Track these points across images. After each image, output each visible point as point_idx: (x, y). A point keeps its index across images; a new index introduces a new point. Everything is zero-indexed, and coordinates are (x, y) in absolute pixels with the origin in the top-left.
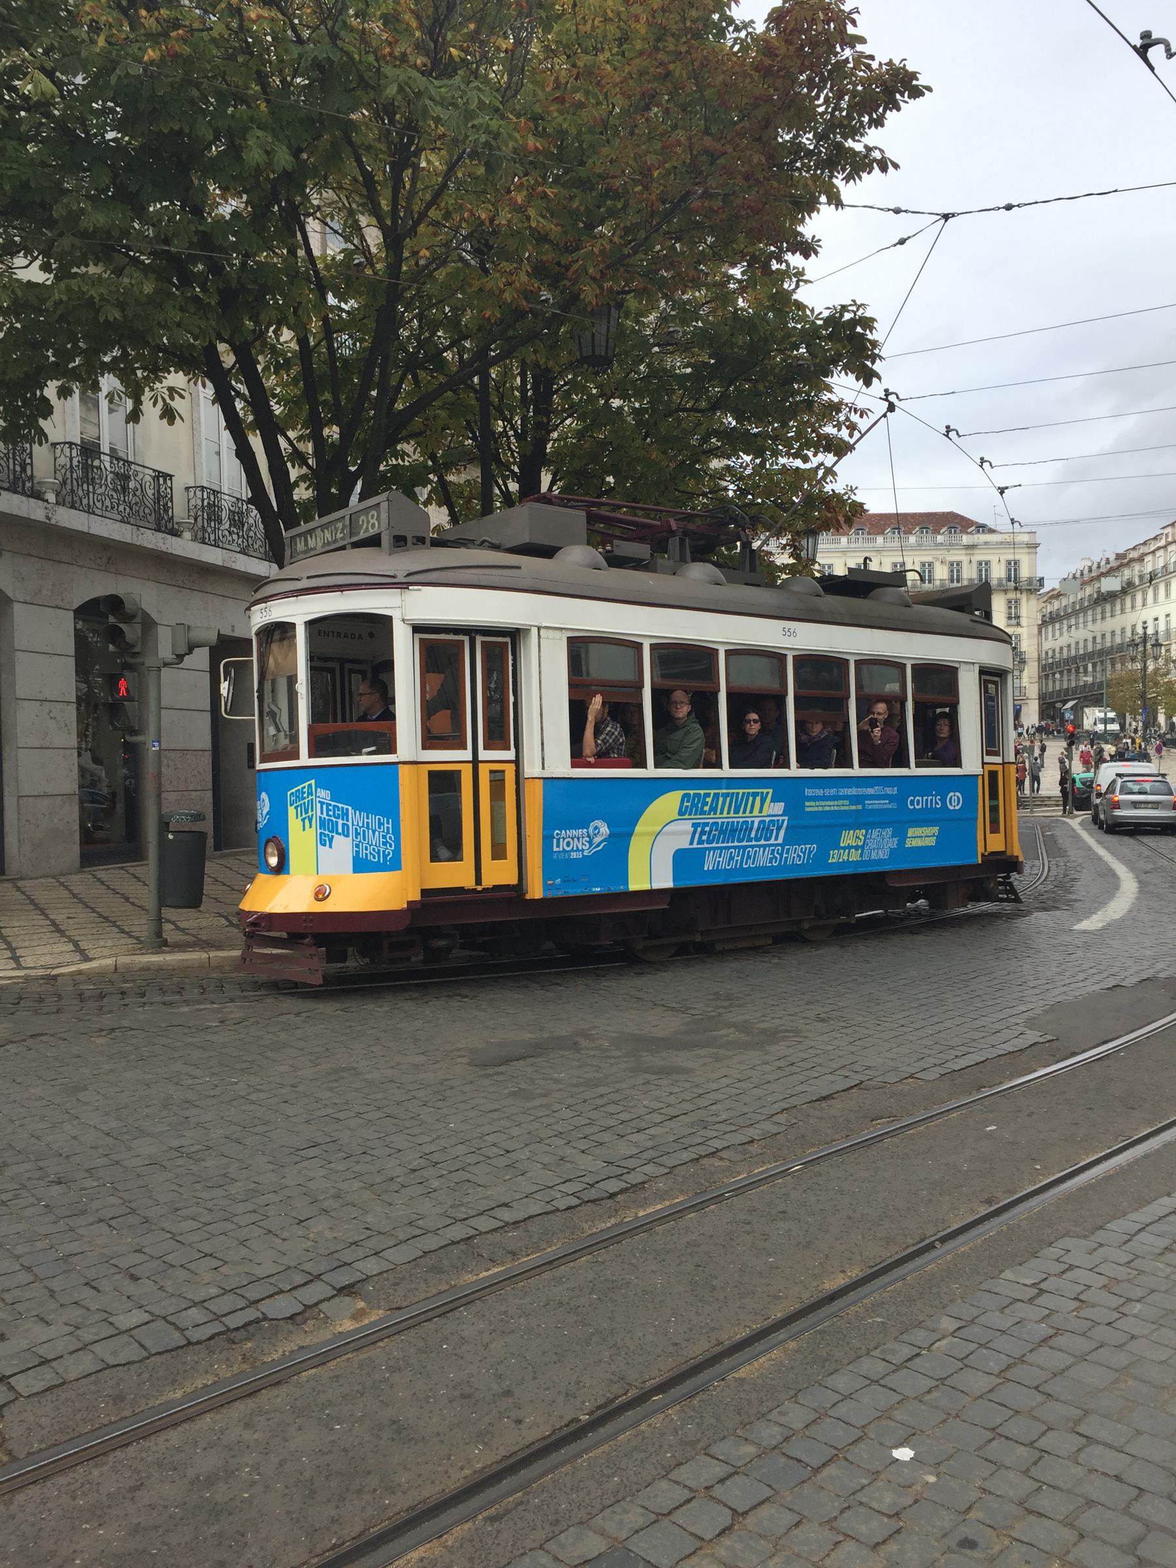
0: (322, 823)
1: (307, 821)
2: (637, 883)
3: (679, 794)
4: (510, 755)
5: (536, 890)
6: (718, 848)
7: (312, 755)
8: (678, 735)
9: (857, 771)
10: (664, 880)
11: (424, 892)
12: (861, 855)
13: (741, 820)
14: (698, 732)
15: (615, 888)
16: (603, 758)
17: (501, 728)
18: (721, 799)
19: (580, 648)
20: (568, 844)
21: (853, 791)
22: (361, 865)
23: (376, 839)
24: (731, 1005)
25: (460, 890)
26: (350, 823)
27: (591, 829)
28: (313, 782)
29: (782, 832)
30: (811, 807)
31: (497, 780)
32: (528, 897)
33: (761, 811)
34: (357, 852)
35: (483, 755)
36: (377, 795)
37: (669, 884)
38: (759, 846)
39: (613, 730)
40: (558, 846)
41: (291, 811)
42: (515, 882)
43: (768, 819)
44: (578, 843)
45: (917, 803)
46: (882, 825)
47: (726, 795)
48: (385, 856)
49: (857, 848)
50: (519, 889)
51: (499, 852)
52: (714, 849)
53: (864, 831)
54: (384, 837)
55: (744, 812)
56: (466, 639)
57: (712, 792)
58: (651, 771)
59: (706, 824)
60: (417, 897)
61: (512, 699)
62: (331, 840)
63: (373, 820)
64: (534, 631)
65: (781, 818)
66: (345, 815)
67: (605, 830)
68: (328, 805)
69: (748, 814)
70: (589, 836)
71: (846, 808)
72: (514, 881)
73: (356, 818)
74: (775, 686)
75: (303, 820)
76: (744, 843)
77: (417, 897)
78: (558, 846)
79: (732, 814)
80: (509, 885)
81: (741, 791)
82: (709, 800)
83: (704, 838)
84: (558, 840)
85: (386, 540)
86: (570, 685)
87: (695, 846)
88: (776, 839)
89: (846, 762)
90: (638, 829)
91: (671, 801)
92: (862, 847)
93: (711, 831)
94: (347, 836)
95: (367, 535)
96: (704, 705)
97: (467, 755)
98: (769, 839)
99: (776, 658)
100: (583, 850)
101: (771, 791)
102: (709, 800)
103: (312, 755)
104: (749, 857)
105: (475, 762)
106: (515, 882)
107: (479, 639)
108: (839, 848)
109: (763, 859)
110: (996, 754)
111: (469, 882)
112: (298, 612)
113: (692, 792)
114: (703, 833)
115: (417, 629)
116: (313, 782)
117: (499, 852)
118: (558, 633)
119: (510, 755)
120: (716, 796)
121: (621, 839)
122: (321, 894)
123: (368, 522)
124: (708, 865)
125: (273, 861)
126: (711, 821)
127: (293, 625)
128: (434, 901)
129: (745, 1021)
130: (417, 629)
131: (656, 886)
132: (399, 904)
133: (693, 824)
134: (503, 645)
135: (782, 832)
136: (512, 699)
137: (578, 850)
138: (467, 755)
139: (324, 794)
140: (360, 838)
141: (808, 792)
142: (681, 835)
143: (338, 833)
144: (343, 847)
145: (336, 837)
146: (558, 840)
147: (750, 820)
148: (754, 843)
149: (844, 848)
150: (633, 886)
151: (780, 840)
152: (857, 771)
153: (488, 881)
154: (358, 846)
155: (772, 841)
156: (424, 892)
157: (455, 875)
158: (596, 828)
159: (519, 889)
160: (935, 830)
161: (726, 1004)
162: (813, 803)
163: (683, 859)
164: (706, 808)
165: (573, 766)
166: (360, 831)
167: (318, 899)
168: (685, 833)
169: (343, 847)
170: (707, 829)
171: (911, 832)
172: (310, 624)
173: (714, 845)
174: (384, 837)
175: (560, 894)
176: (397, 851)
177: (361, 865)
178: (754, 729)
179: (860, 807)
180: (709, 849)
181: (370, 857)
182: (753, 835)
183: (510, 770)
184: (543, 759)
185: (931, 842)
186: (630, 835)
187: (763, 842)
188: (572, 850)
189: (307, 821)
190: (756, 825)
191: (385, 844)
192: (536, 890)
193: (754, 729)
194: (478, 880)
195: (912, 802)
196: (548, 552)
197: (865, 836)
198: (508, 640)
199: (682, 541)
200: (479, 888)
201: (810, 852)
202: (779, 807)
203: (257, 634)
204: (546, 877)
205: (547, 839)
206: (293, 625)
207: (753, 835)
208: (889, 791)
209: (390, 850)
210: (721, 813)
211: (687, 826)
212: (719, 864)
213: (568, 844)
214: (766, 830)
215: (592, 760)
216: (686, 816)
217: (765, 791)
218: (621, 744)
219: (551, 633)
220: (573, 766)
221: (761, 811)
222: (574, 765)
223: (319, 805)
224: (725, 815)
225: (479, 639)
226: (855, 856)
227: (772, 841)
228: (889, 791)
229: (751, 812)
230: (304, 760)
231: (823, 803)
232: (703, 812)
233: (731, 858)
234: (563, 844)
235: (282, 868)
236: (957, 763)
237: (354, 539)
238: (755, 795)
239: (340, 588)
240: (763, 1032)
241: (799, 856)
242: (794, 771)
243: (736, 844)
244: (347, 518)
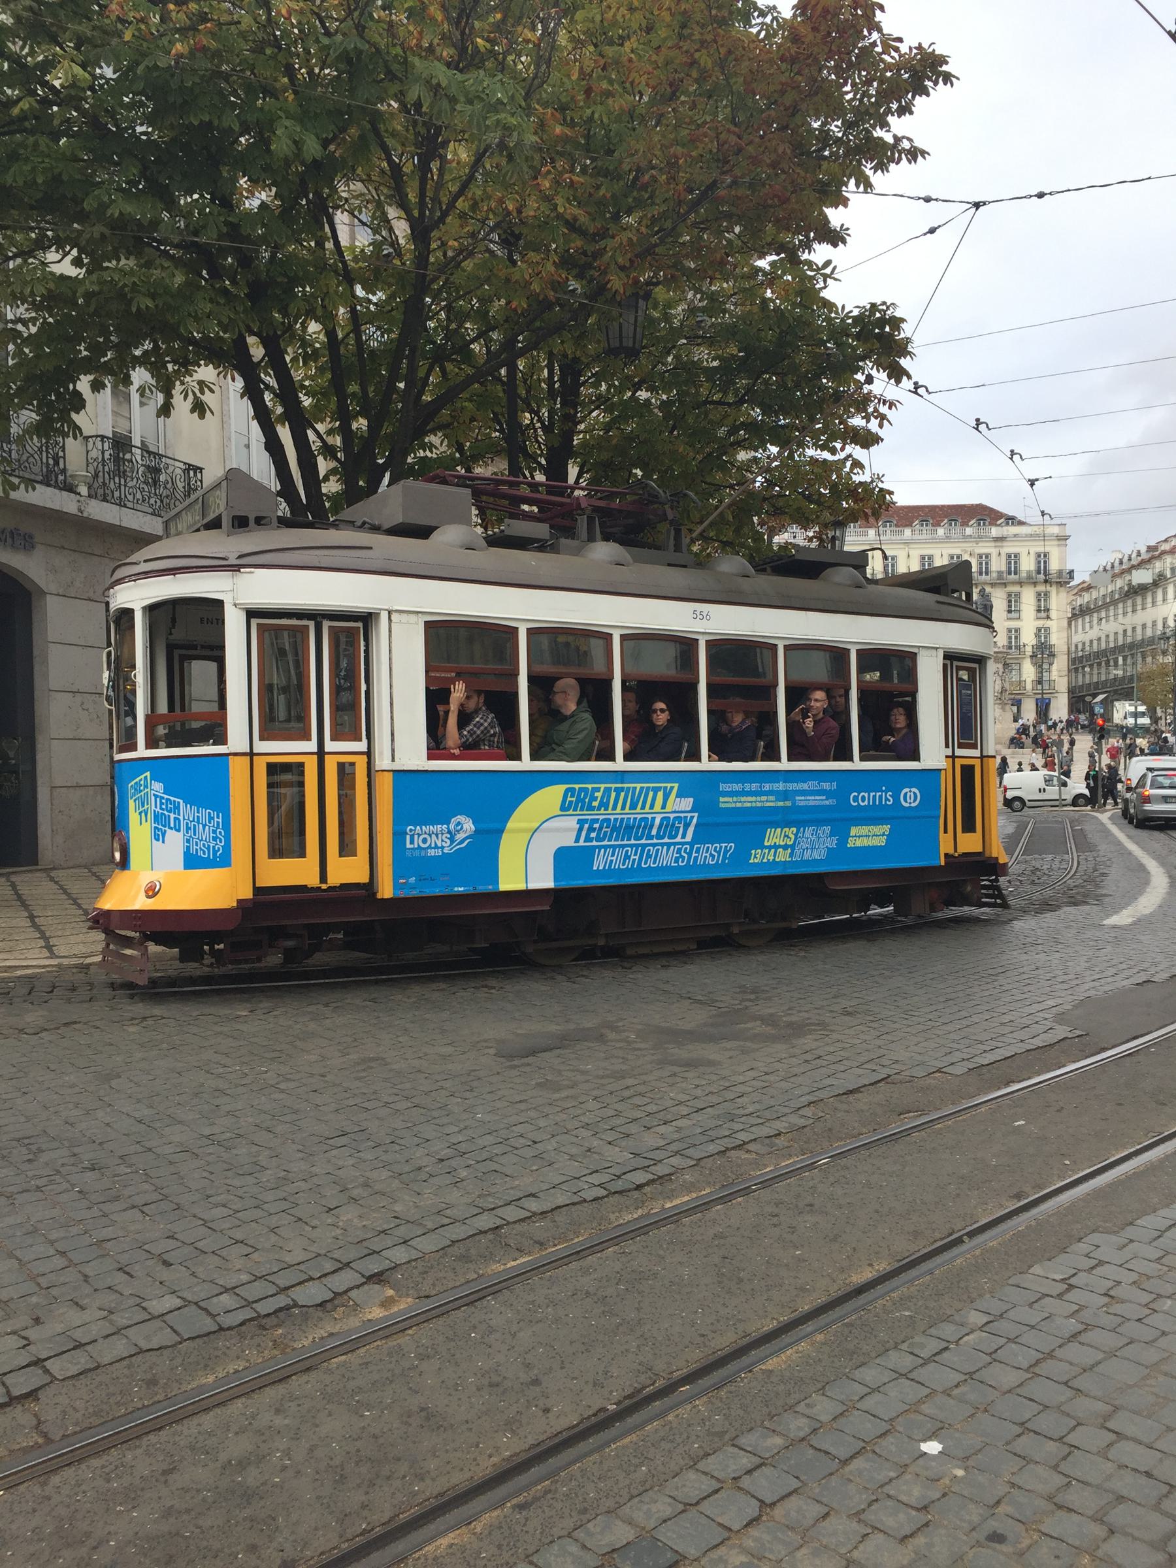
0: (157, 817)
2: (510, 880)
3: (560, 789)
4: (362, 746)
5: (386, 890)
6: (610, 846)
8: (565, 726)
9: (784, 764)
10: (543, 880)
12: (791, 855)
13: (640, 816)
14: (587, 721)
15: (482, 888)
18: (613, 794)
20: (425, 841)
21: (781, 786)
22: (192, 861)
23: (206, 833)
24: (757, 999)
25: (303, 888)
26: (181, 818)
27: (452, 826)
28: (148, 774)
29: (691, 831)
30: (726, 802)
31: (345, 773)
32: (379, 896)
33: (663, 807)
34: (188, 848)
35: (330, 746)
37: (550, 884)
38: (662, 845)
39: (485, 721)
40: (412, 842)
41: (131, 803)
42: (367, 880)
43: (672, 816)
45: (862, 799)
46: (818, 823)
47: (618, 791)
48: (215, 852)
49: (785, 847)
50: (369, 888)
51: (347, 848)
52: (606, 847)
53: (794, 829)
54: (214, 832)
55: (643, 807)
56: (311, 624)
57: (603, 786)
58: (526, 763)
59: (596, 821)
60: (248, 894)
61: (364, 687)
62: (164, 834)
63: (204, 813)
65: (689, 815)
66: (177, 808)
67: (469, 826)
68: (162, 798)
69: (647, 810)
70: (449, 832)
71: (772, 804)
72: (364, 878)
73: (187, 812)
74: (684, 677)
75: (140, 813)
76: (643, 841)
77: (248, 894)
78: (412, 842)
79: (627, 810)
80: (358, 884)
81: (638, 786)
82: (599, 795)
83: (593, 835)
84: (412, 837)
85: (225, 522)
87: (581, 843)
88: (684, 836)
89: (773, 755)
90: (509, 825)
91: (553, 795)
92: (792, 847)
93: (600, 829)
94: (179, 830)
96: (595, 693)
98: (675, 836)
99: (685, 645)
100: (443, 847)
101: (676, 785)
102: (599, 795)
104: (649, 856)
105: (321, 753)
106: (367, 880)
107: (326, 624)
108: (763, 847)
109: (667, 858)
110: (974, 746)
111: (313, 880)
113: (577, 786)
114: (591, 829)
116: (148, 774)
118: (413, 618)
119: (362, 746)
120: (608, 790)
124: (599, 864)
126: (601, 817)
127: (132, 611)
129: (772, 1015)
130: (251, 614)
131: (531, 886)
133: (579, 821)
134: (353, 630)
135: (691, 831)
136: (364, 687)
137: (436, 847)
138: (311, 746)
139: (158, 787)
140: (191, 832)
141: (724, 787)
142: (565, 832)
143: (170, 828)
144: (175, 841)
145: (169, 831)
146: (412, 837)
147: (650, 816)
148: (655, 841)
149: (770, 848)
150: (504, 886)
151: (689, 838)
152: (784, 764)
153: (334, 879)
154: (188, 841)
155: (678, 839)
157: (296, 872)
158: (459, 823)
159: (369, 888)
160: (886, 828)
161: (752, 997)
162: (730, 799)
163: (562, 856)
164: (595, 804)
165: (429, 759)
166: (191, 825)
167: (149, 897)
169: (175, 841)
170: (596, 826)
171: (854, 831)
173: (605, 843)
174: (214, 832)
175: (415, 893)
176: (227, 847)
177: (192, 861)
178: (661, 719)
179: (789, 804)
180: (600, 847)
181: (200, 853)
182: (654, 832)
184: (393, 750)
185: (881, 841)
186: (501, 831)
187: (666, 840)
188: (430, 847)
190: (657, 822)
191: (215, 839)
192: (386, 890)
193: (661, 719)
194: (323, 877)
195: (856, 799)
196: (423, 532)
197: (796, 835)
198: (360, 624)
199: (590, 521)
200: (324, 886)
201: (726, 851)
202: (687, 803)
204: (396, 876)
205: (399, 836)
206: (132, 611)
207: (654, 832)
208: (826, 786)
210: (614, 808)
211: (571, 823)
212: (611, 863)
213: (425, 841)
214: (670, 827)
215: (457, 752)
216: (571, 812)
217: (669, 785)
218: (494, 735)
219: (404, 617)
220: (429, 759)
221: (663, 807)
222: (430, 757)
224: (618, 810)
225: (326, 624)
226: (783, 856)
227: (678, 839)
228: (826, 786)
229: (652, 807)
231: (743, 799)
232: (590, 808)
233: (627, 857)
234: (418, 841)
235: (124, 864)
236: (916, 756)
238: (659, 789)
240: (790, 1025)
241: (711, 855)
242: (706, 763)
243: (633, 842)
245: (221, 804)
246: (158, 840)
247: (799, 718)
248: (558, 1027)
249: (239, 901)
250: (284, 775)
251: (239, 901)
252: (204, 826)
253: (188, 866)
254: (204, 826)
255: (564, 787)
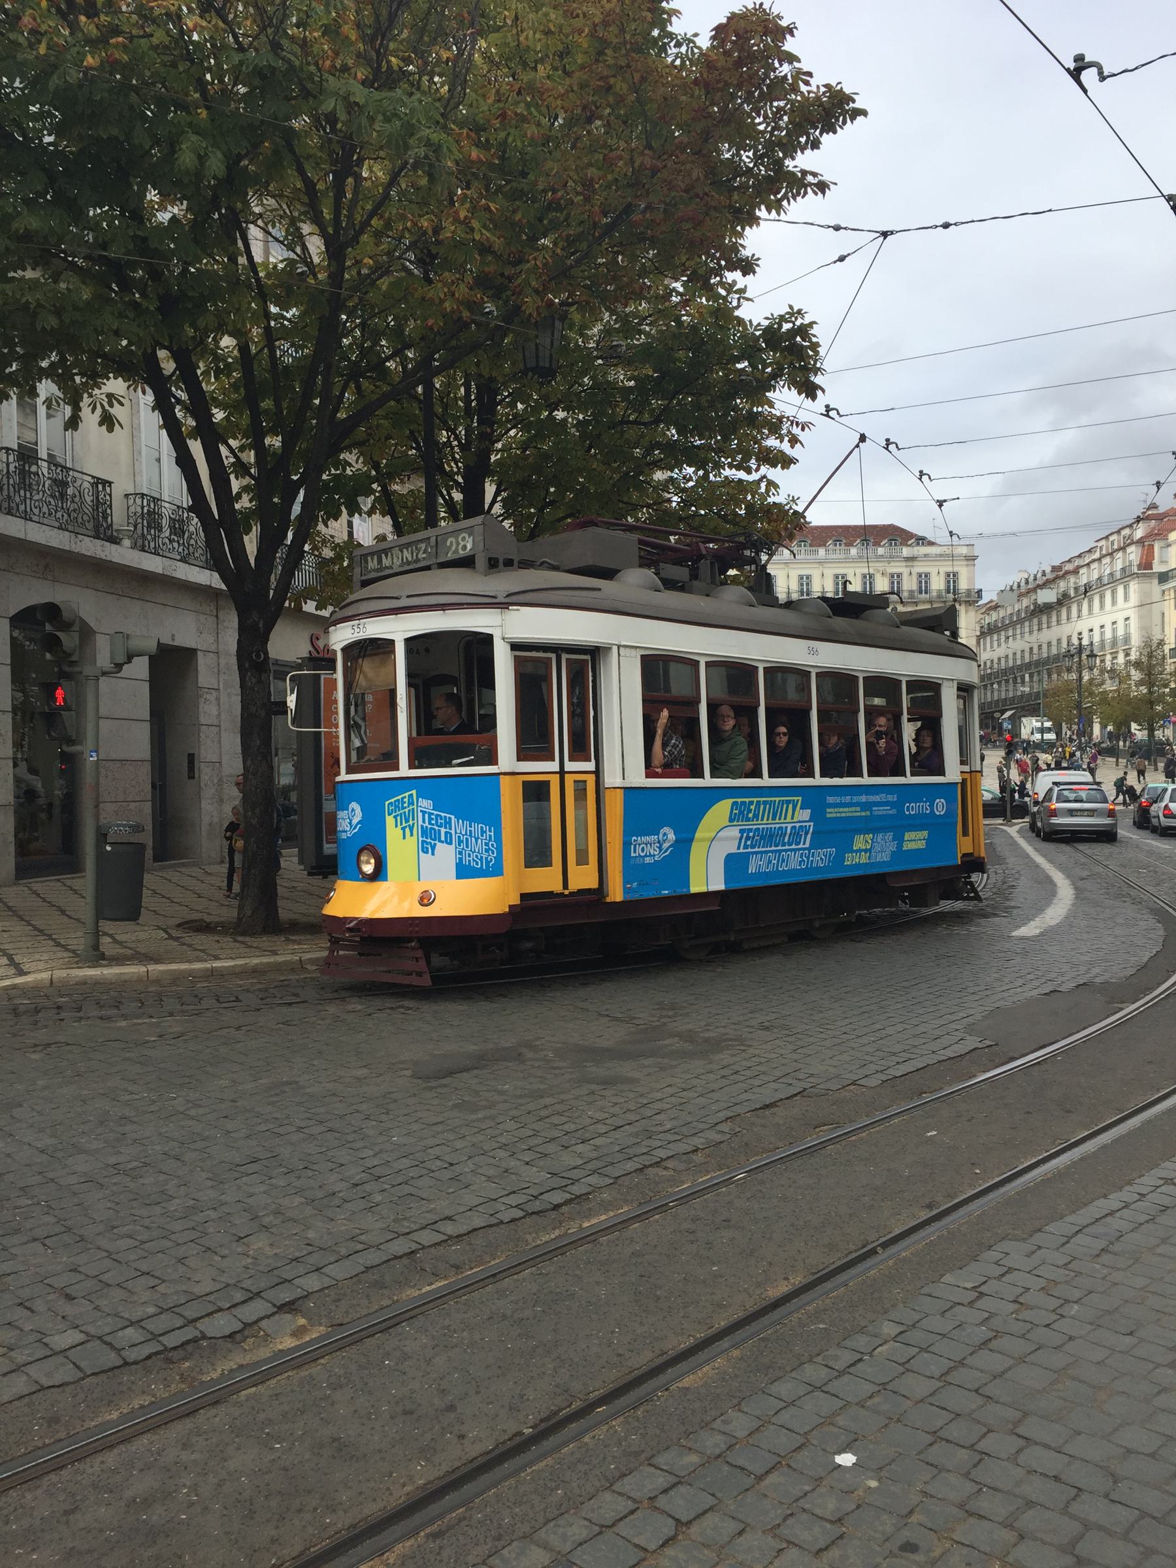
0: (424, 832)
1: (407, 830)
2: (697, 887)
5: (616, 893)
7: (412, 766)
11: (523, 896)
15: (681, 891)
16: (668, 770)
17: (584, 742)
19: (656, 667)
20: (643, 850)
23: (480, 846)
25: (550, 894)
26: (453, 832)
28: (414, 792)
32: (608, 900)
35: (570, 766)
36: (477, 804)
37: (721, 887)
41: (390, 821)
44: (653, 847)
48: (488, 863)
54: (487, 844)
56: (553, 656)
57: (755, 800)
58: (708, 781)
63: (477, 828)
64: (615, 649)
66: (448, 823)
67: (672, 836)
68: (430, 814)
72: (593, 883)
73: (458, 827)
75: (403, 829)
77: (516, 900)
80: (590, 889)
81: (777, 799)
82: (752, 807)
83: (749, 843)
85: (481, 562)
86: (644, 701)
87: (741, 850)
91: (722, 810)
94: (450, 843)
95: (456, 556)
97: (554, 766)
102: (752, 807)
103: (412, 766)
105: (562, 773)
107: (564, 657)
109: (794, 862)
111: (557, 887)
112: (398, 629)
113: (739, 800)
114: (748, 838)
115: (515, 646)
116: (414, 792)
117: (582, 860)
118: (633, 651)
119: (590, 766)
121: (684, 844)
122: (425, 899)
123: (458, 544)
125: (368, 868)
127: (392, 642)
128: (532, 905)
129: (690, 1031)
130: (515, 646)
132: (498, 907)
134: (586, 661)
137: (650, 855)
138: (554, 766)
139: (426, 804)
140: (463, 845)
143: (440, 841)
144: (446, 854)
145: (439, 844)
150: (695, 889)
153: (574, 886)
154: (460, 853)
156: (523, 896)
157: (546, 880)
158: (665, 834)
161: (671, 1013)
163: (733, 863)
164: (751, 815)
168: (732, 838)
169: (446, 854)
172: (408, 641)
175: (637, 897)
177: (464, 871)
183: (591, 780)
186: (691, 840)
189: (407, 830)
192: (616, 893)
194: (565, 886)
196: (608, 574)
198: (588, 657)
200: (566, 892)
202: (806, 814)
203: (343, 649)
204: (625, 882)
205: (627, 845)
206: (392, 642)
209: (492, 856)
211: (734, 832)
213: (643, 850)
215: (659, 770)
222: (647, 776)
223: (420, 815)
225: (564, 657)
230: (404, 770)
232: (748, 820)
234: (639, 849)
237: (441, 560)
238: (788, 802)
239: (443, 607)
240: (707, 1040)
244: (433, 540)
245: (494, 820)
246: (427, 852)
247: (872, 739)
248: (473, 1047)
249: (510, 906)
250: (535, 792)
251: (510, 906)
252: (477, 839)
253: (460, 876)
254: (477, 839)
255: (731, 801)
